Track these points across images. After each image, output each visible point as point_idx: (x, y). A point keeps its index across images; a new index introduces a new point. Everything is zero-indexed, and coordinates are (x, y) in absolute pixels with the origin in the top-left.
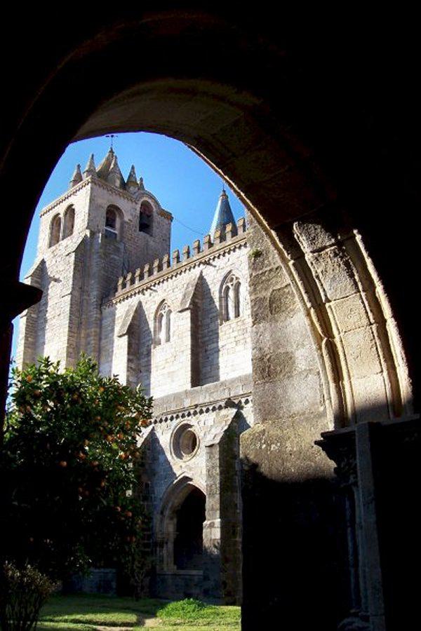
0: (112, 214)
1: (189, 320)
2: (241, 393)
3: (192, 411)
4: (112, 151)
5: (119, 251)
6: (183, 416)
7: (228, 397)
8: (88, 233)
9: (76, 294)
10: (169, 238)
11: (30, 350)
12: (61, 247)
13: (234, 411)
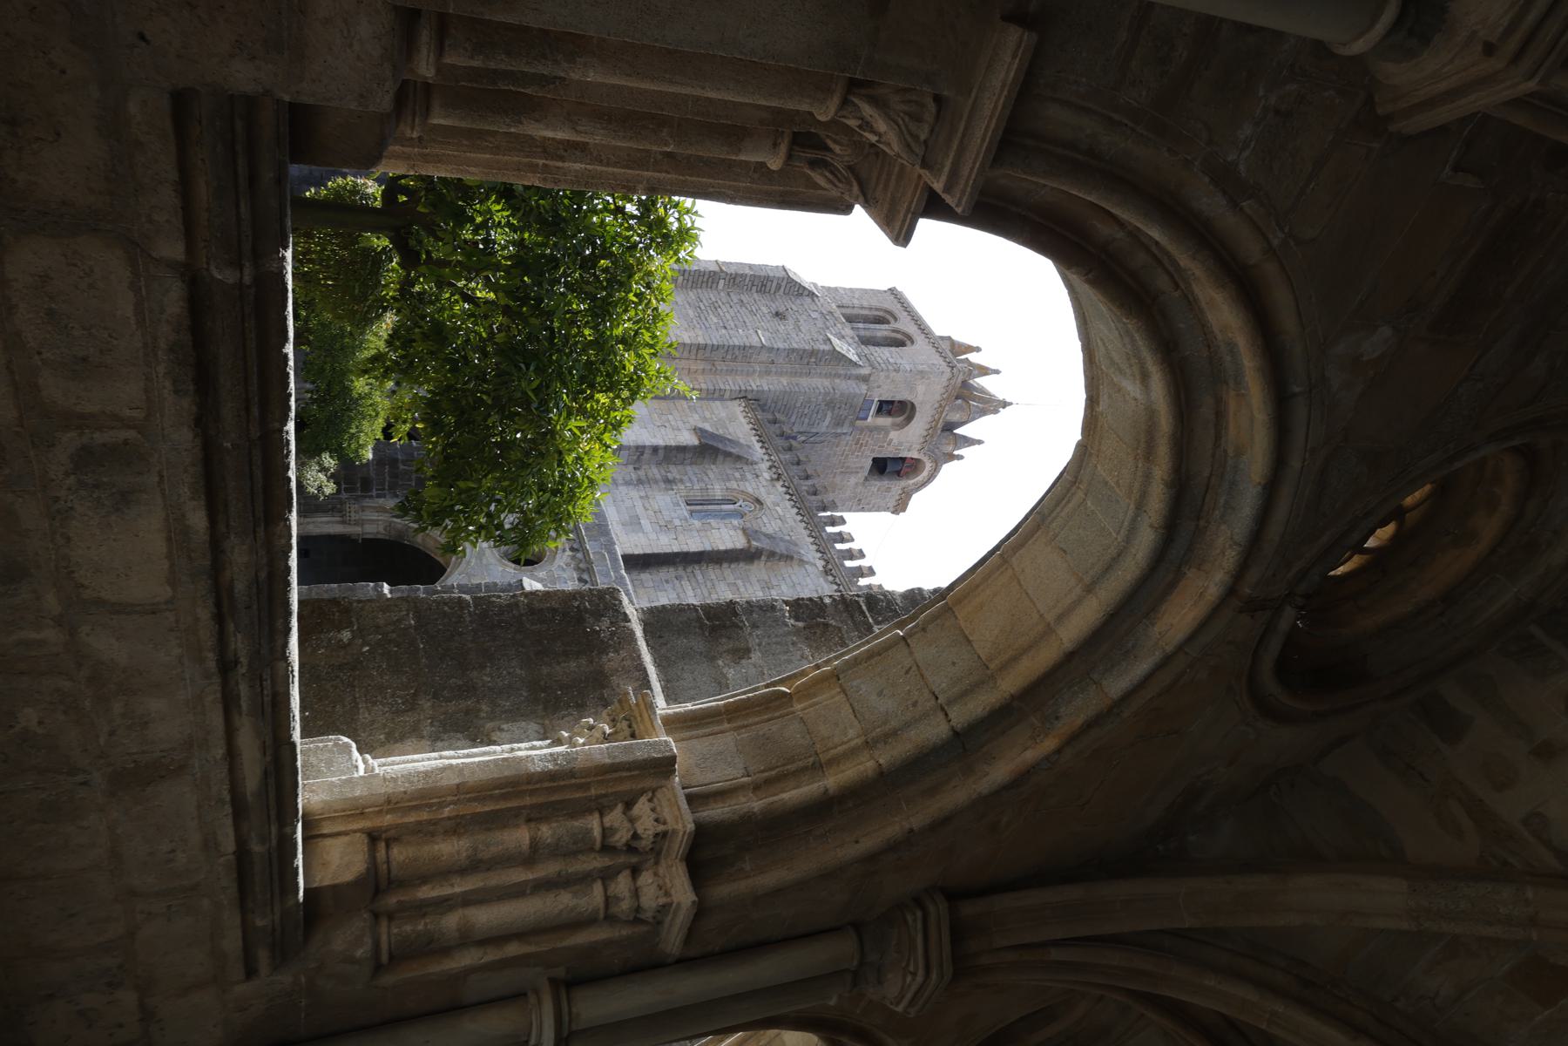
0: (897, 409)
1: (729, 546)
4: (1005, 404)
5: (838, 424)
10: (863, 510)
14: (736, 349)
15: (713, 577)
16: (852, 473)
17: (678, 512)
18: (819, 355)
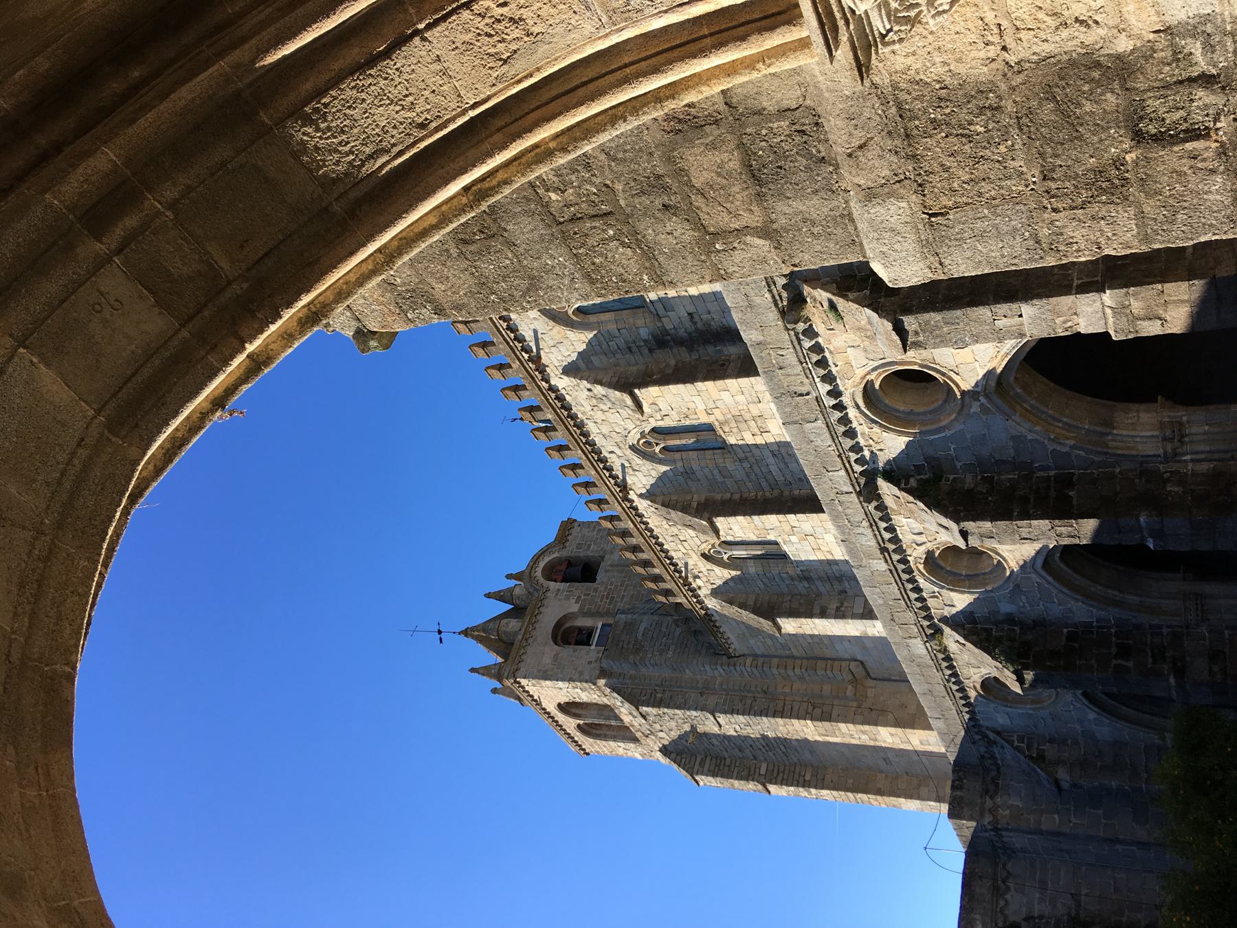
1: (731, 519)
2: (843, 473)
3: (896, 557)
4: (466, 633)
6: (909, 571)
7: (854, 495)
8: (602, 682)
9: (712, 701)
11: (828, 777)
12: (636, 724)
13: (881, 483)
14: (741, 710)
15: (749, 485)
16: (617, 566)
17: (794, 549)
18: (652, 699)
